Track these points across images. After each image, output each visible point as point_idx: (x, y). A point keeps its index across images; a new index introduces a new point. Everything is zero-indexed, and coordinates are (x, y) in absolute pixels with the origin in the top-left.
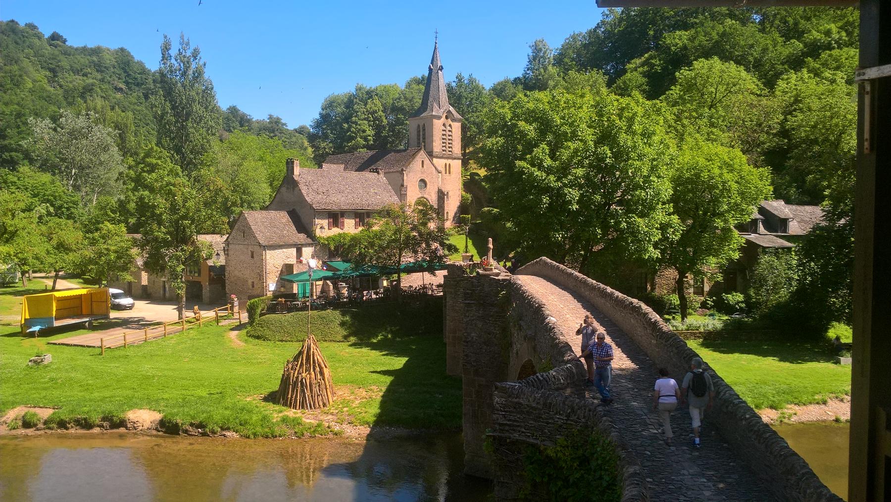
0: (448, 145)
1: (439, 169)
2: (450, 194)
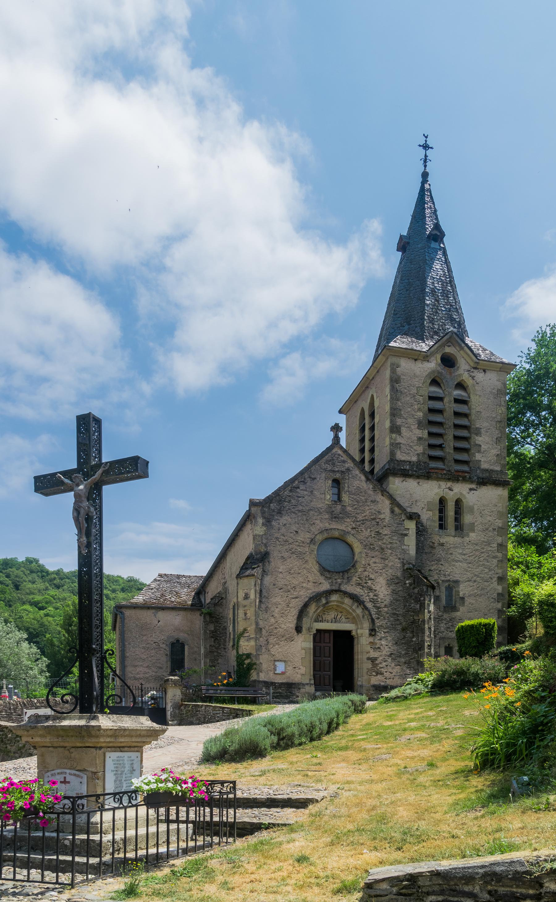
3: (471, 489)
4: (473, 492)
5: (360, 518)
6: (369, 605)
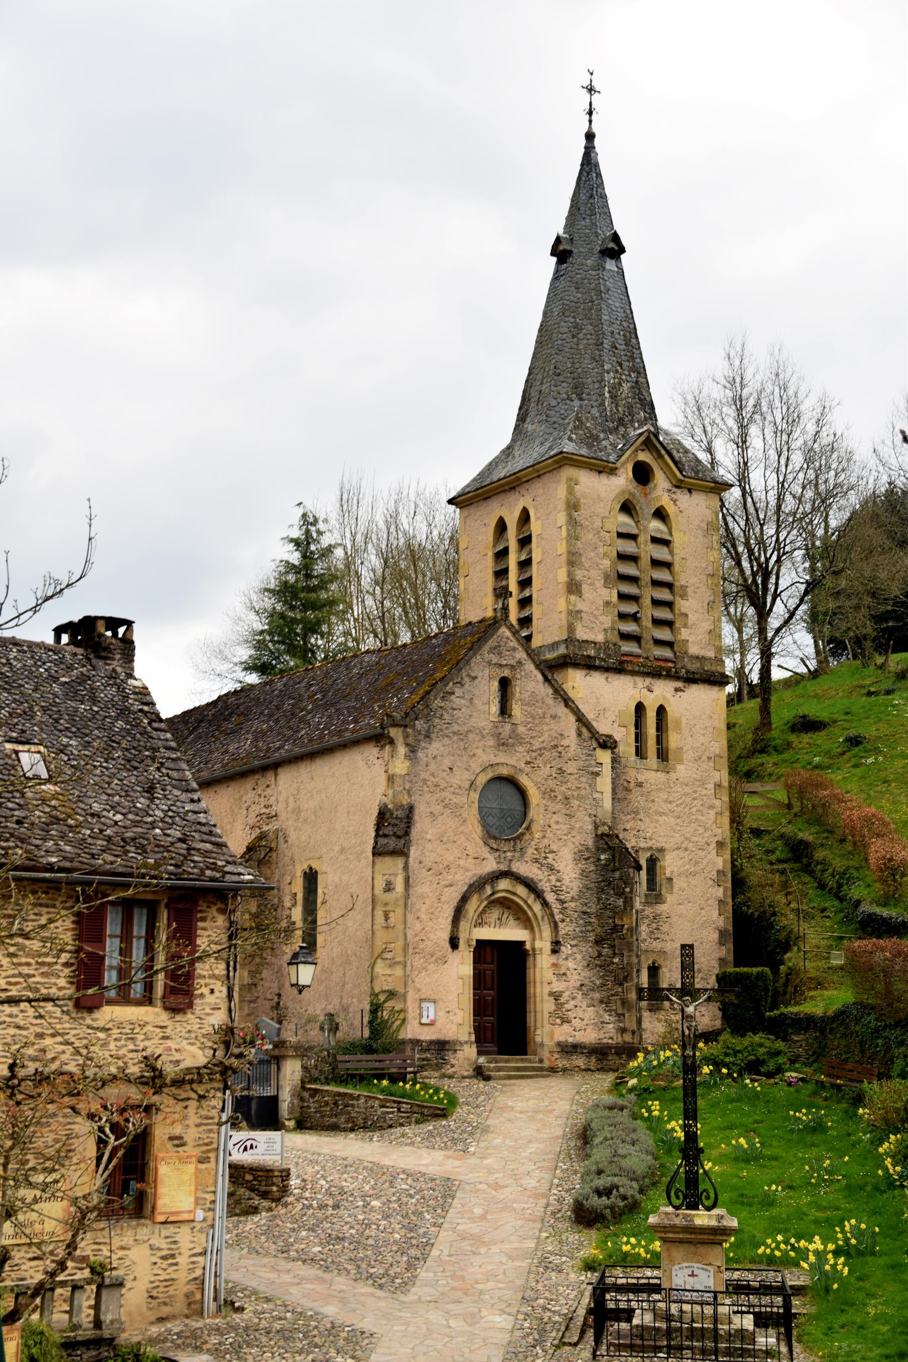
0: (648, 612)
1: (603, 727)
2: (670, 865)
3: (677, 690)
4: (679, 693)
5: (536, 745)
6: (550, 897)
